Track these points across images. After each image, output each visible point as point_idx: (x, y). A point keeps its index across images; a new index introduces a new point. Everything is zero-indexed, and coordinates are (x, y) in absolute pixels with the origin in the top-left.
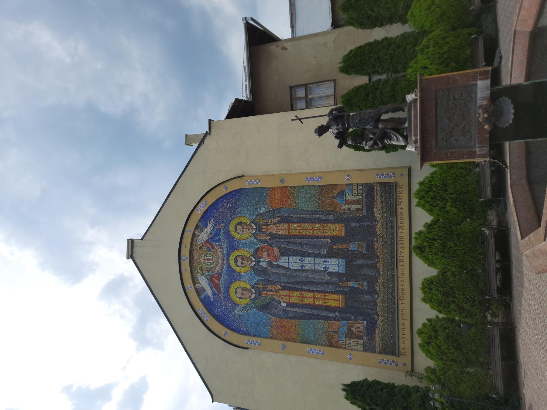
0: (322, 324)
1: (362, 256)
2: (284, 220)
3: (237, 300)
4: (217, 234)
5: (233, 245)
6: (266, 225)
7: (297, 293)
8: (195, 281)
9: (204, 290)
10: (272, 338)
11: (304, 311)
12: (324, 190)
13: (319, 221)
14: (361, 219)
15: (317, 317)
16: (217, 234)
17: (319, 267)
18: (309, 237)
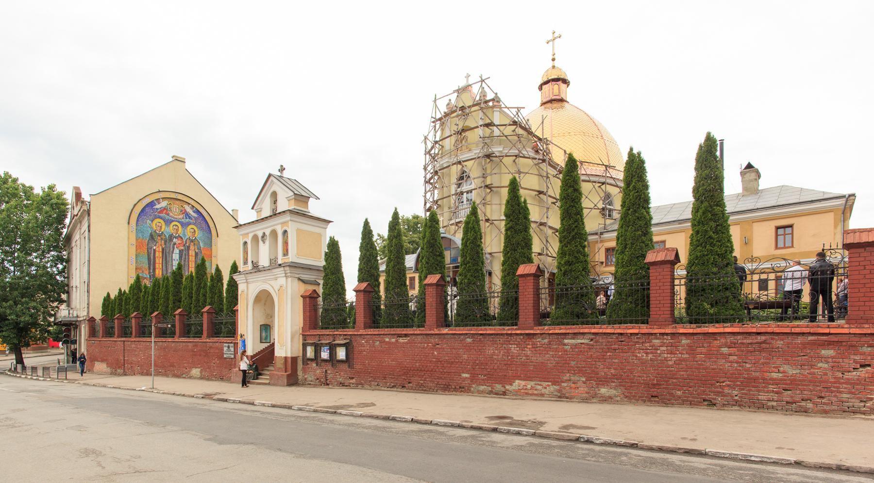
4: (190, 218)
10: (137, 240)
15: (149, 264)
16: (190, 218)
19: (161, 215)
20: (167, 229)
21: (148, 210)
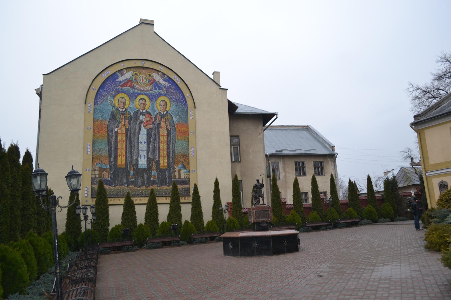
0: (106, 154)
1: (149, 178)
2: (169, 132)
3: (117, 98)
5: (153, 98)
6: (166, 121)
7: (124, 138)
8: (128, 69)
9: (122, 75)
10: (94, 121)
11: (113, 143)
12: (186, 158)
13: (168, 154)
14: (170, 178)
15: (110, 150)
16: (160, 88)
17: (141, 153)
18: (159, 147)
19: (125, 88)
20: (132, 105)
21: (109, 83)
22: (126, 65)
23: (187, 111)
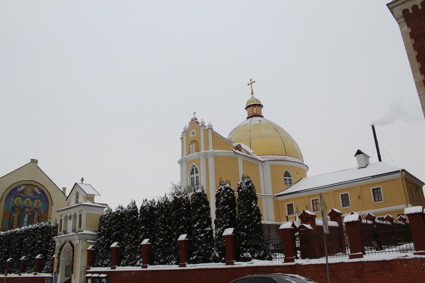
2: (38, 217)
3: (16, 199)
5: (33, 200)
8: (23, 185)
10: (4, 211)
16: (37, 195)
22: (22, 183)
23: (48, 207)
